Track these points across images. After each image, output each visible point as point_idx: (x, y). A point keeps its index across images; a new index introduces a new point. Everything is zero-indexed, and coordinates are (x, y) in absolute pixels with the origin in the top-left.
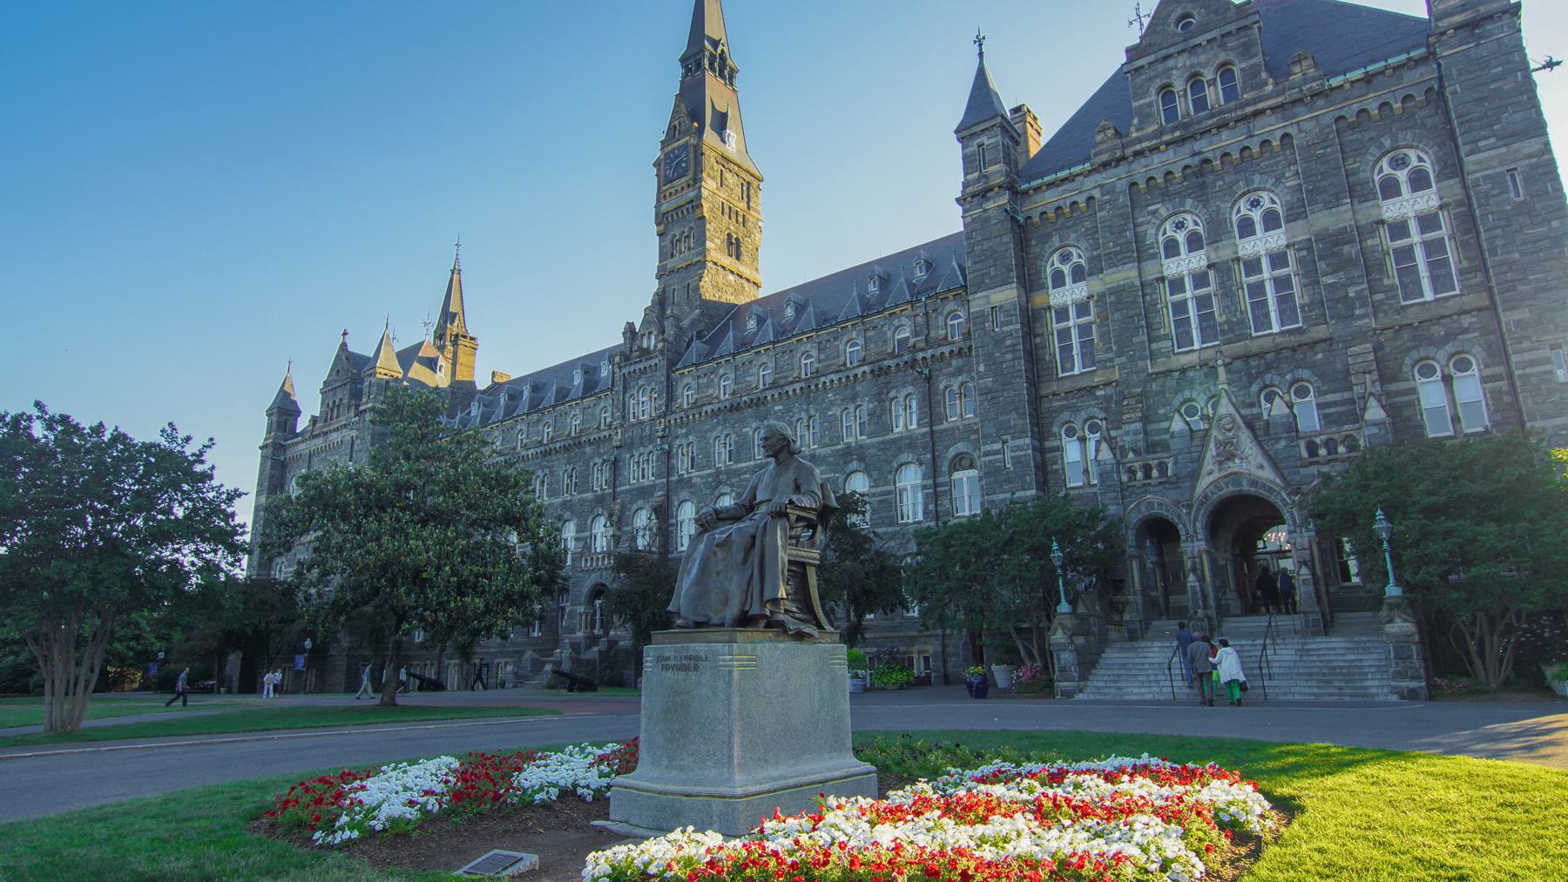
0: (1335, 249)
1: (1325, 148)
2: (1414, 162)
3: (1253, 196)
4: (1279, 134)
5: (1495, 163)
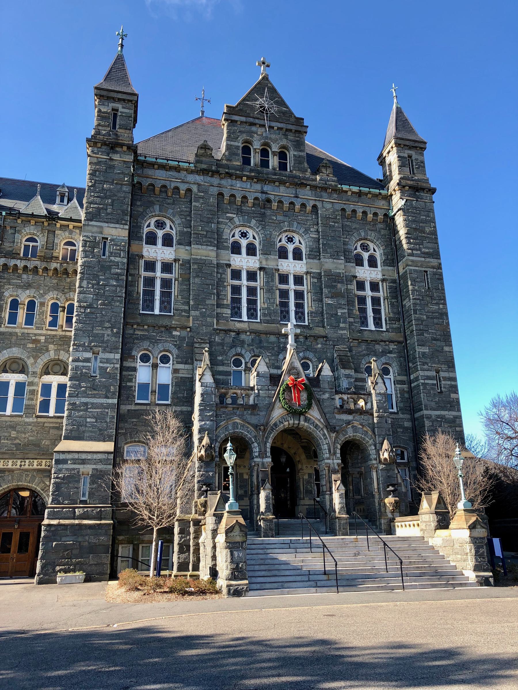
0: (334, 284)
1: (335, 222)
2: (372, 251)
3: (290, 234)
4: (312, 203)
5: (419, 265)
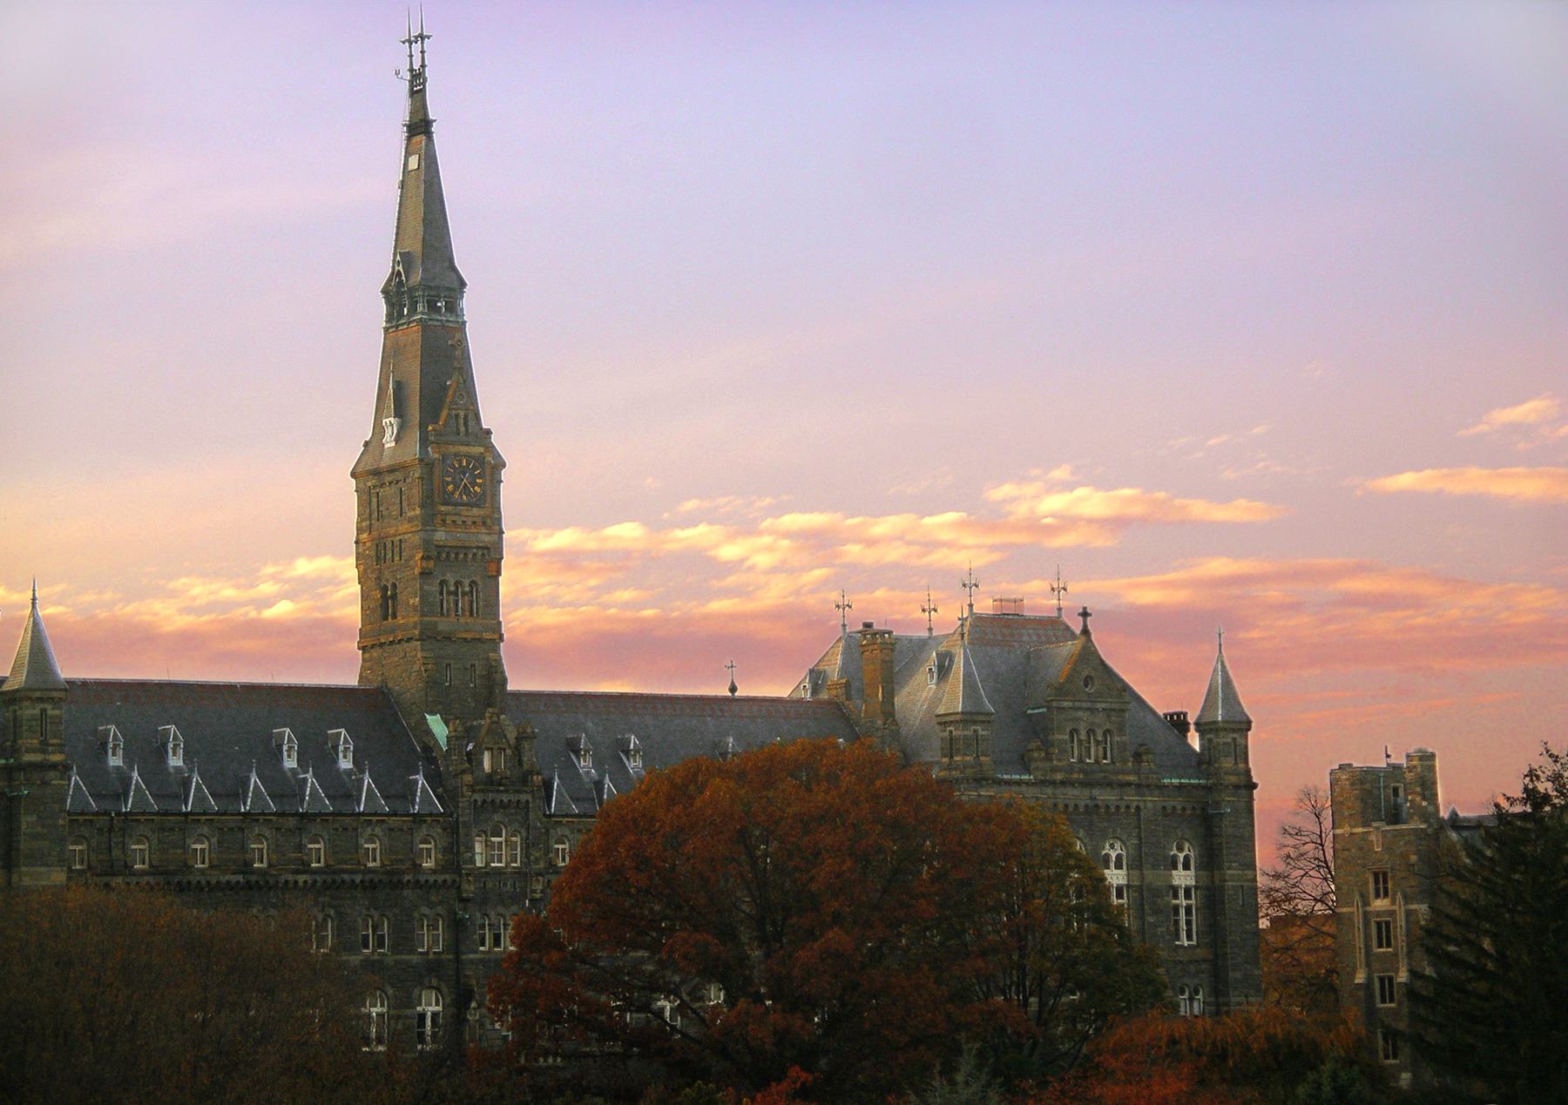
1: (1156, 825)
4: (1135, 804)
5: (1236, 879)
